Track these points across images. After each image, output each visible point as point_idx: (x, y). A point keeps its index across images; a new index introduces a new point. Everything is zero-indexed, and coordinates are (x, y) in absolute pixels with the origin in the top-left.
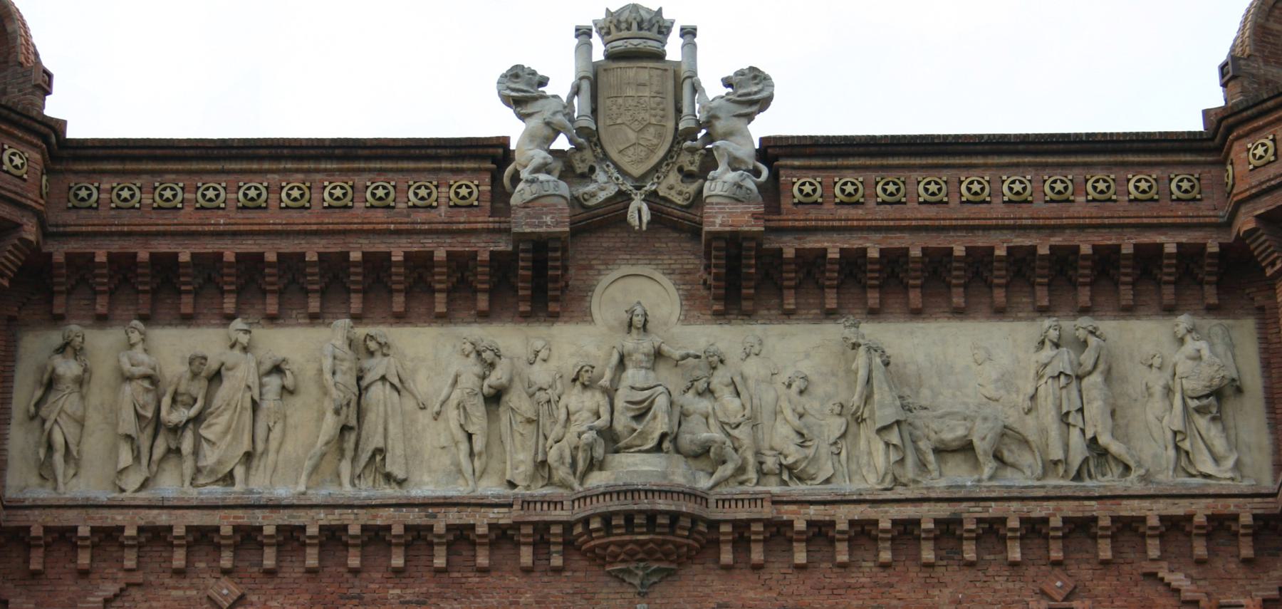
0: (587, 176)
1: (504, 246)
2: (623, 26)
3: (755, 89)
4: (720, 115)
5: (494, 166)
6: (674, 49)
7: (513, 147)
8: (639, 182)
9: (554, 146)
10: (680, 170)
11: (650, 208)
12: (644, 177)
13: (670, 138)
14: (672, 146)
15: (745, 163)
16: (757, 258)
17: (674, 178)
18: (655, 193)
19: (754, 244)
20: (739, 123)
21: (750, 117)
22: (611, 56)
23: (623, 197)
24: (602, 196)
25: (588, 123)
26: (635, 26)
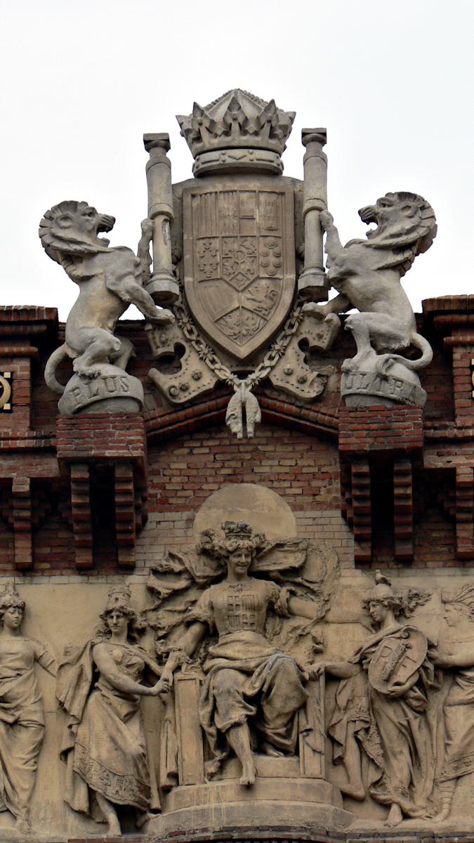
0: (171, 362)
1: (49, 468)
2: (220, 129)
3: (408, 225)
4: (358, 269)
5: (35, 349)
6: (293, 161)
7: (63, 318)
8: (243, 367)
9: (126, 316)
10: (303, 344)
11: (261, 405)
12: (253, 359)
13: (287, 297)
14: (291, 309)
15: (396, 338)
16: (416, 485)
17: (293, 359)
18: (265, 383)
19: (408, 466)
20: (387, 279)
21: (401, 268)
22: (201, 174)
23: (223, 389)
24: (195, 389)
25: (165, 284)
26: (235, 127)
